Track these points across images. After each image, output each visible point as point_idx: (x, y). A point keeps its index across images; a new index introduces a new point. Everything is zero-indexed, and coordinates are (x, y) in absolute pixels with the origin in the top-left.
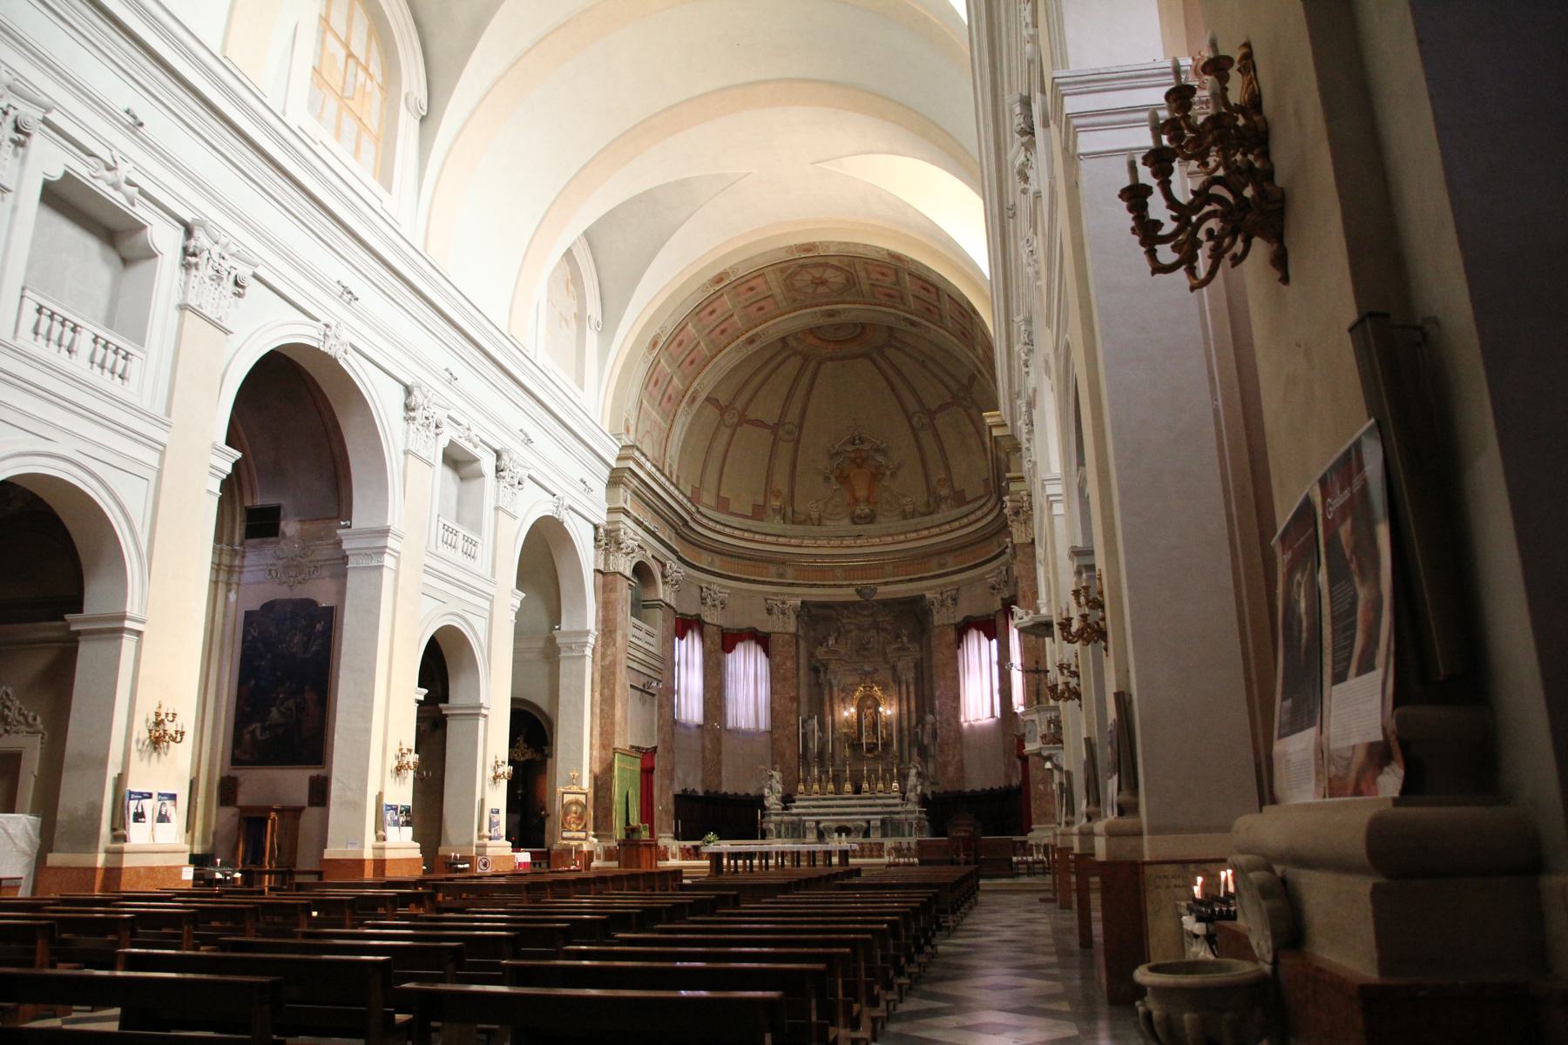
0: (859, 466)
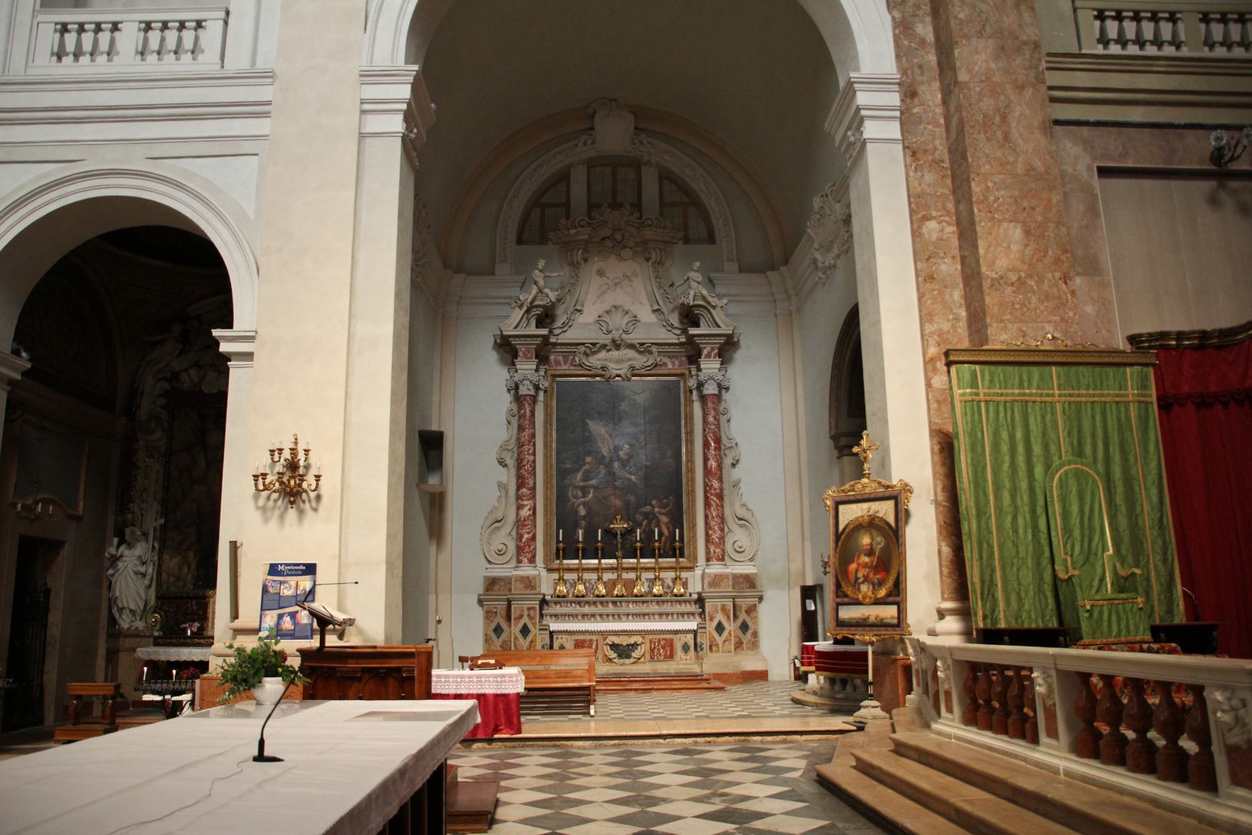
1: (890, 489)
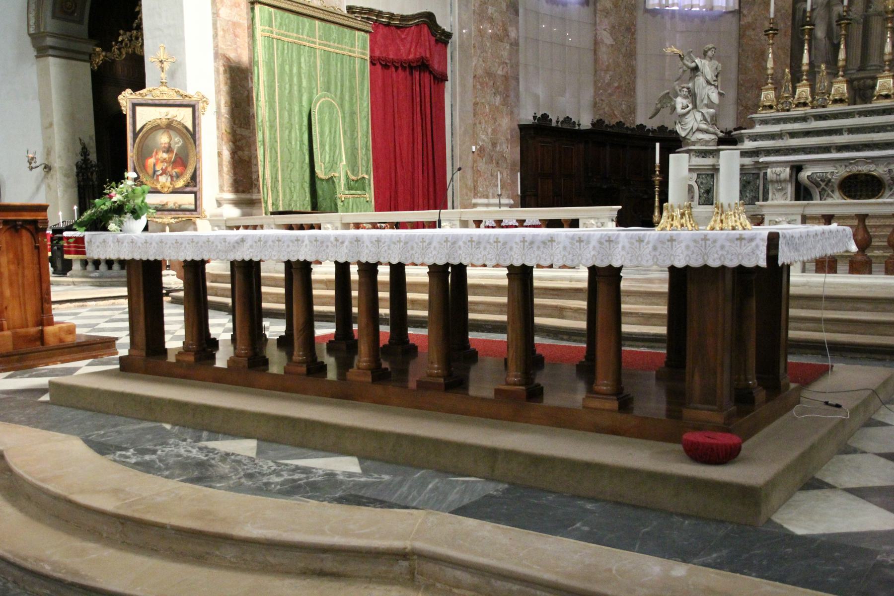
1: (187, 99)
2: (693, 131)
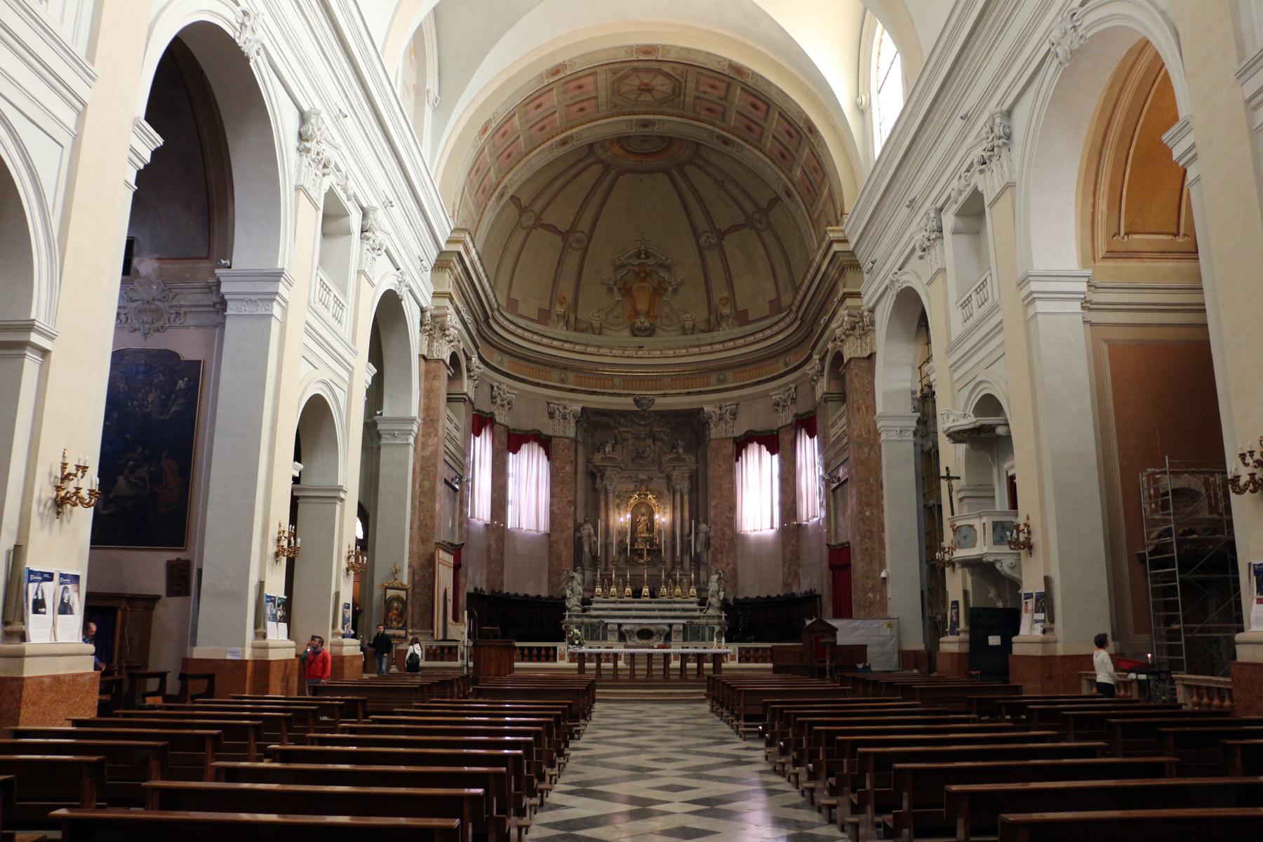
0: (643, 280)
2: (573, 606)
